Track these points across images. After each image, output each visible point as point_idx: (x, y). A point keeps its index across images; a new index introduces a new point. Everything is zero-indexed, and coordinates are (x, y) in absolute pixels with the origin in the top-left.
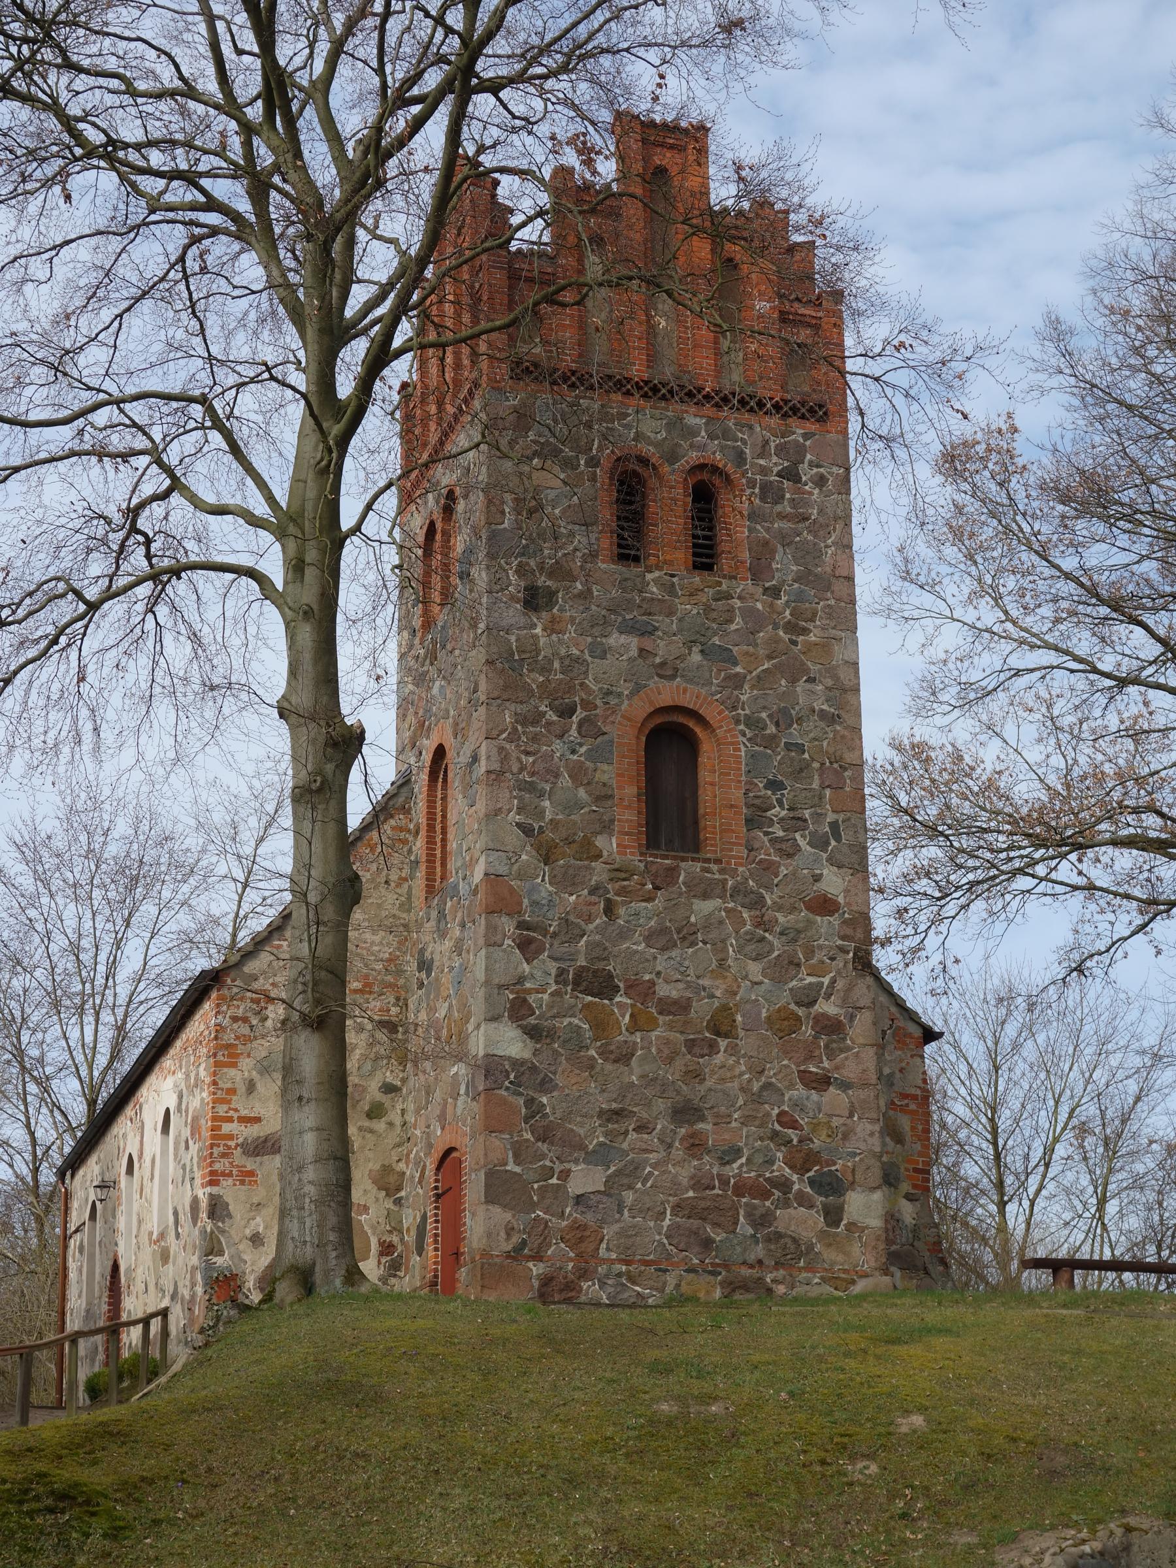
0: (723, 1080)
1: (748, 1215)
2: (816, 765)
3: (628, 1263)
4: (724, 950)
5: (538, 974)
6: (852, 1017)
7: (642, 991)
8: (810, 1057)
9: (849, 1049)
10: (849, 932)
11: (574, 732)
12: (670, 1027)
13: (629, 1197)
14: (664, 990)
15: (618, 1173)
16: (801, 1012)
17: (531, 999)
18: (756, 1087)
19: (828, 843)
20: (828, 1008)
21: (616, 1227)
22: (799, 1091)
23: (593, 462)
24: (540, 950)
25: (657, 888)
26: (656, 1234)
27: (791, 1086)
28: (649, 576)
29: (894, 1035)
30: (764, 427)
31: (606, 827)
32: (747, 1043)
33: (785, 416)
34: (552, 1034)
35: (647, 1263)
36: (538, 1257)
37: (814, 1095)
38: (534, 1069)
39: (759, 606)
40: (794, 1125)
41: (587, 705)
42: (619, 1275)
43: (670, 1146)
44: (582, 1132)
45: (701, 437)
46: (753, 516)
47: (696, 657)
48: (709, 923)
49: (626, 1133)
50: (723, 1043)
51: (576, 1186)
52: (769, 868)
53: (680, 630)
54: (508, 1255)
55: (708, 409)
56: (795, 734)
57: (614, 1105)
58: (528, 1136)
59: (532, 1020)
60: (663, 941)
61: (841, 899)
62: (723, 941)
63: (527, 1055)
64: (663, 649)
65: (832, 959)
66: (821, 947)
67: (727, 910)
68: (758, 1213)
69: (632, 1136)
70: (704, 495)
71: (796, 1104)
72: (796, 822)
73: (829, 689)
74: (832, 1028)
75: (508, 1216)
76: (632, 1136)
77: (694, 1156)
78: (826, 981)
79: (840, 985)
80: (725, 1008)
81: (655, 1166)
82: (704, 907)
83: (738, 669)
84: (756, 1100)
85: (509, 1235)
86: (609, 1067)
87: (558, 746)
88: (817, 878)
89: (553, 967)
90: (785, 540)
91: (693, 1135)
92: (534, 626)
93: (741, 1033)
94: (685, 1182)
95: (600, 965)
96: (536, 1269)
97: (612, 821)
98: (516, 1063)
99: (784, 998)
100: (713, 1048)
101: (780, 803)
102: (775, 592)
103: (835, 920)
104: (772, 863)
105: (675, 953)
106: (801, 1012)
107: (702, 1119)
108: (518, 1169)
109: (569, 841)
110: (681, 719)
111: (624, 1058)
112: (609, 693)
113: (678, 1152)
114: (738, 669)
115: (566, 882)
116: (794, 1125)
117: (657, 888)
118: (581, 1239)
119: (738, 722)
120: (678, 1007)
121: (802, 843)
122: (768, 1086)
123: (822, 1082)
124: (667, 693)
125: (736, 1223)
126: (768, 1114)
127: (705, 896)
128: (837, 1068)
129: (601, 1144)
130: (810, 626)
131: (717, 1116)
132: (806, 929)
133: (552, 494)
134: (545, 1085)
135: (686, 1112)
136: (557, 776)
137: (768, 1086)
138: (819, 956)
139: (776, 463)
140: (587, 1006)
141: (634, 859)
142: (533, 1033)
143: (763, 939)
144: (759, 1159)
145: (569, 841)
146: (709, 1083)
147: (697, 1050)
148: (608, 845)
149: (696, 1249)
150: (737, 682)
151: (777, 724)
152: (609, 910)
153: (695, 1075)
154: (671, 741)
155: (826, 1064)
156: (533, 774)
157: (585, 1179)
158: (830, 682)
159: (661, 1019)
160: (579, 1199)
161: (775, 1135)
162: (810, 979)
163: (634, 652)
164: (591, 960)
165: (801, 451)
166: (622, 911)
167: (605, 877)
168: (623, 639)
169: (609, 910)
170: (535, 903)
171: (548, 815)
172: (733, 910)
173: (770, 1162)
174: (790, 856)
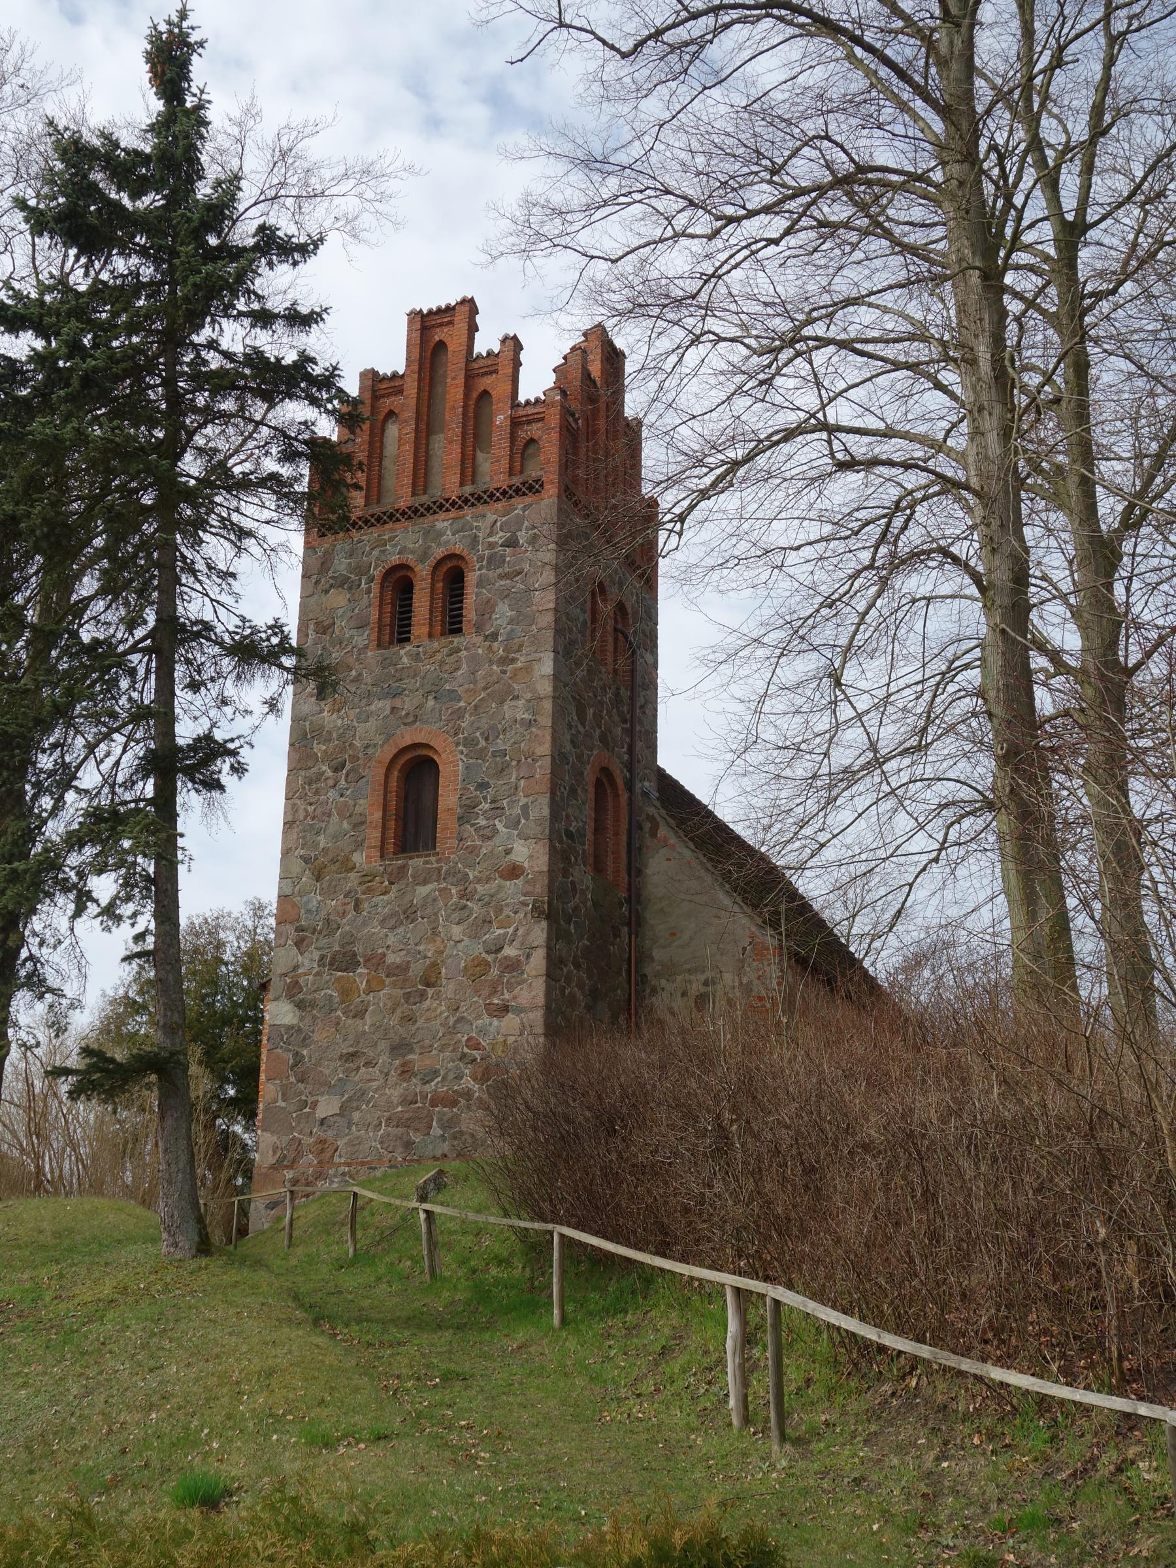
0: (428, 1020)
1: (440, 1120)
2: (514, 763)
3: (348, 1165)
4: (437, 920)
5: (306, 963)
6: (528, 956)
7: (376, 961)
8: (494, 992)
9: (525, 981)
10: (529, 888)
11: (343, 781)
12: (394, 985)
13: (356, 1116)
14: (391, 958)
15: (350, 1099)
16: (490, 958)
17: (301, 981)
18: (452, 1020)
19: (519, 822)
20: (509, 951)
21: (345, 1140)
22: (486, 1019)
23: (371, 580)
24: (308, 946)
25: (391, 883)
26: (372, 1141)
27: (478, 1017)
28: (402, 652)
29: (753, 949)
30: (491, 514)
31: (359, 845)
32: (448, 990)
33: (511, 497)
34: (313, 1004)
35: (362, 1164)
36: (291, 1167)
37: (495, 1022)
38: (299, 1030)
39: (480, 651)
40: (477, 1047)
41: (354, 758)
42: (343, 1174)
43: (387, 1074)
44: (327, 1072)
45: (448, 533)
46: (480, 584)
47: (431, 703)
48: (427, 901)
49: (358, 1068)
50: (430, 991)
51: (321, 1113)
52: (473, 850)
53: (422, 686)
54: (272, 1167)
55: (453, 513)
56: (500, 744)
57: (351, 1050)
58: (293, 1079)
59: (301, 996)
60: (393, 922)
61: (526, 865)
62: (436, 914)
63: (295, 1022)
64: (407, 704)
65: (516, 913)
66: (507, 905)
67: (440, 890)
68: (446, 1118)
69: (363, 1070)
70: (453, 576)
71: (482, 1031)
72: (497, 810)
73: (529, 701)
74: (513, 966)
75: (275, 1138)
76: (363, 1070)
77: (404, 1080)
78: (511, 930)
79: (520, 933)
80: (434, 965)
81: (376, 1091)
82: (423, 891)
83: (462, 704)
84: (452, 1031)
85: (275, 1153)
86: (350, 1021)
87: (332, 794)
88: (508, 852)
89: (316, 955)
90: (505, 595)
91: (403, 1065)
92: (322, 711)
93: (444, 982)
94: (395, 1100)
95: (349, 948)
96: (289, 1174)
97: (363, 841)
98: (289, 1028)
99: (478, 949)
100: (423, 996)
101: (485, 798)
102: (494, 636)
103: (519, 882)
104: (475, 847)
105: (400, 930)
106: (490, 958)
107: (411, 1051)
108: (283, 1104)
109: (334, 861)
110: (424, 752)
111: (360, 1014)
112: (367, 747)
113: (393, 1077)
114: (462, 704)
115: (330, 892)
116: (477, 1047)
117: (391, 883)
118: (322, 1151)
119: (458, 744)
120: (401, 970)
121: (499, 826)
122: (461, 1020)
123: (505, 1009)
124: (408, 737)
125: (430, 1127)
126: (459, 1041)
127: (425, 882)
128: (515, 998)
129: (340, 1080)
130: (517, 655)
131: (422, 1047)
132: (497, 892)
133: (340, 611)
134: (305, 1042)
135: (400, 1048)
136: (330, 815)
137: (461, 1020)
138: (506, 912)
139: (499, 537)
140: (338, 979)
141: (376, 865)
142: (300, 1005)
143: (465, 906)
144: (451, 1076)
145: (334, 861)
146: (418, 1024)
147: (412, 1000)
148: (358, 858)
149: (400, 1150)
150: (459, 714)
151: (487, 739)
152: (357, 906)
153: (410, 1019)
154: (416, 771)
155: (507, 996)
156: (313, 818)
157: (327, 1106)
158: (529, 696)
159: (388, 980)
160: (322, 1122)
161: (464, 1056)
162: (501, 931)
163: (388, 712)
164: (342, 946)
165: (519, 521)
166: (366, 905)
167: (356, 882)
168: (380, 704)
169: (357, 906)
170: (309, 911)
171: (322, 845)
172: (445, 889)
173: (459, 1077)
174: (489, 838)
